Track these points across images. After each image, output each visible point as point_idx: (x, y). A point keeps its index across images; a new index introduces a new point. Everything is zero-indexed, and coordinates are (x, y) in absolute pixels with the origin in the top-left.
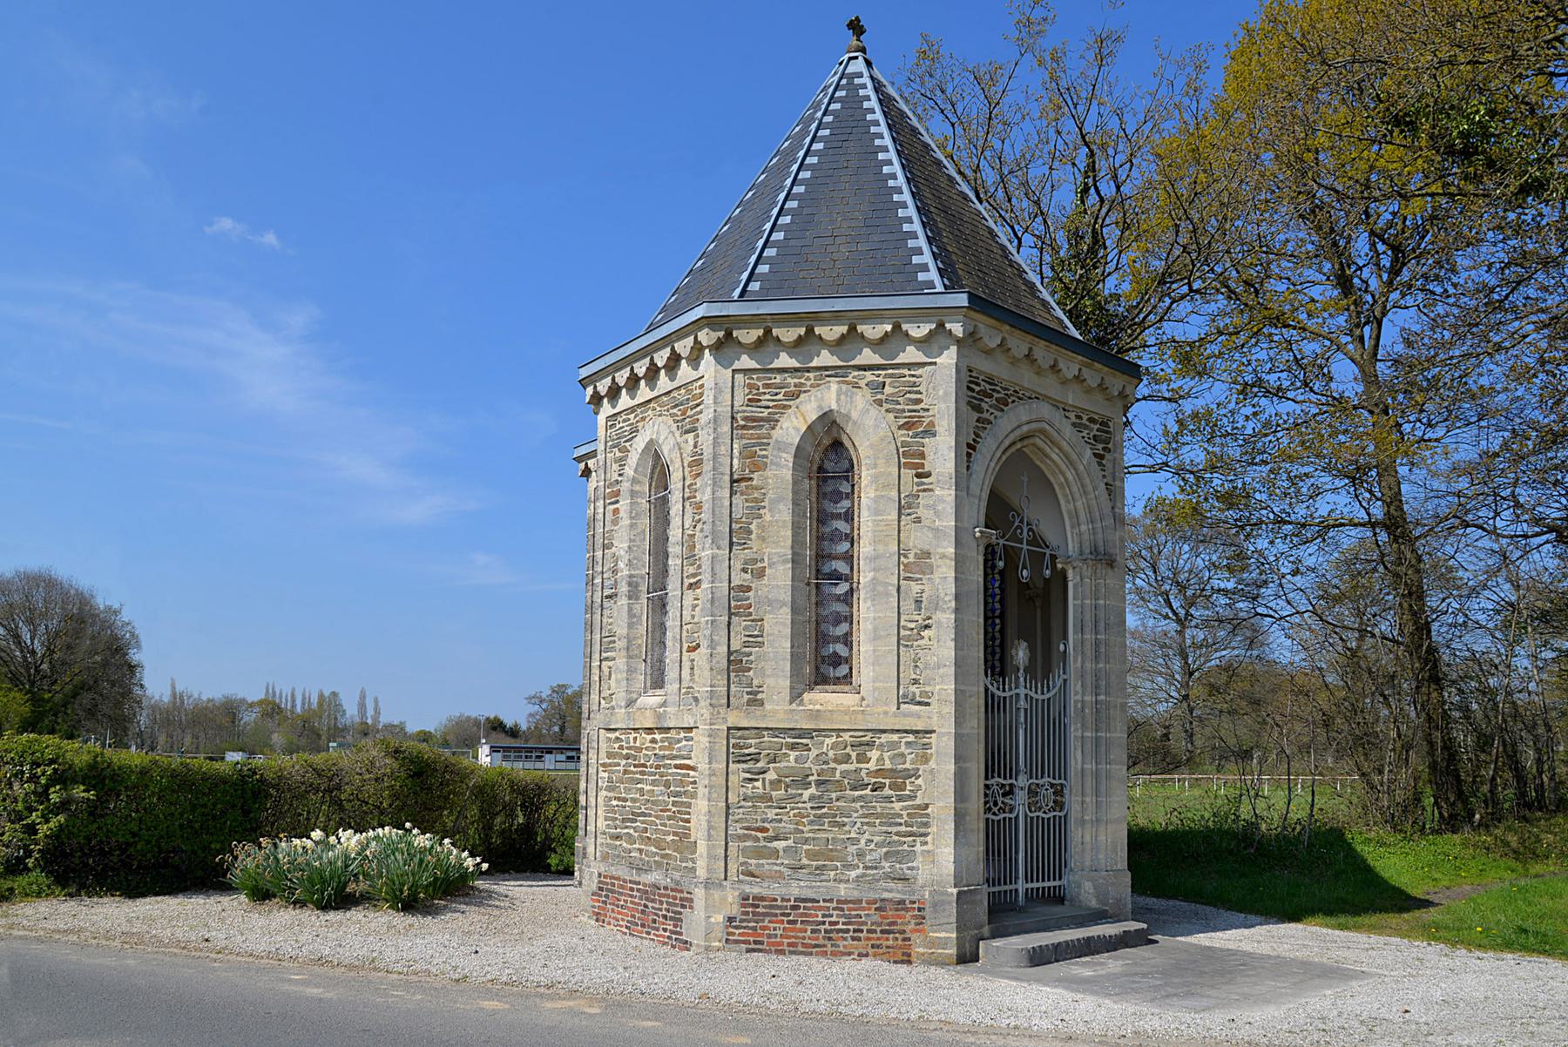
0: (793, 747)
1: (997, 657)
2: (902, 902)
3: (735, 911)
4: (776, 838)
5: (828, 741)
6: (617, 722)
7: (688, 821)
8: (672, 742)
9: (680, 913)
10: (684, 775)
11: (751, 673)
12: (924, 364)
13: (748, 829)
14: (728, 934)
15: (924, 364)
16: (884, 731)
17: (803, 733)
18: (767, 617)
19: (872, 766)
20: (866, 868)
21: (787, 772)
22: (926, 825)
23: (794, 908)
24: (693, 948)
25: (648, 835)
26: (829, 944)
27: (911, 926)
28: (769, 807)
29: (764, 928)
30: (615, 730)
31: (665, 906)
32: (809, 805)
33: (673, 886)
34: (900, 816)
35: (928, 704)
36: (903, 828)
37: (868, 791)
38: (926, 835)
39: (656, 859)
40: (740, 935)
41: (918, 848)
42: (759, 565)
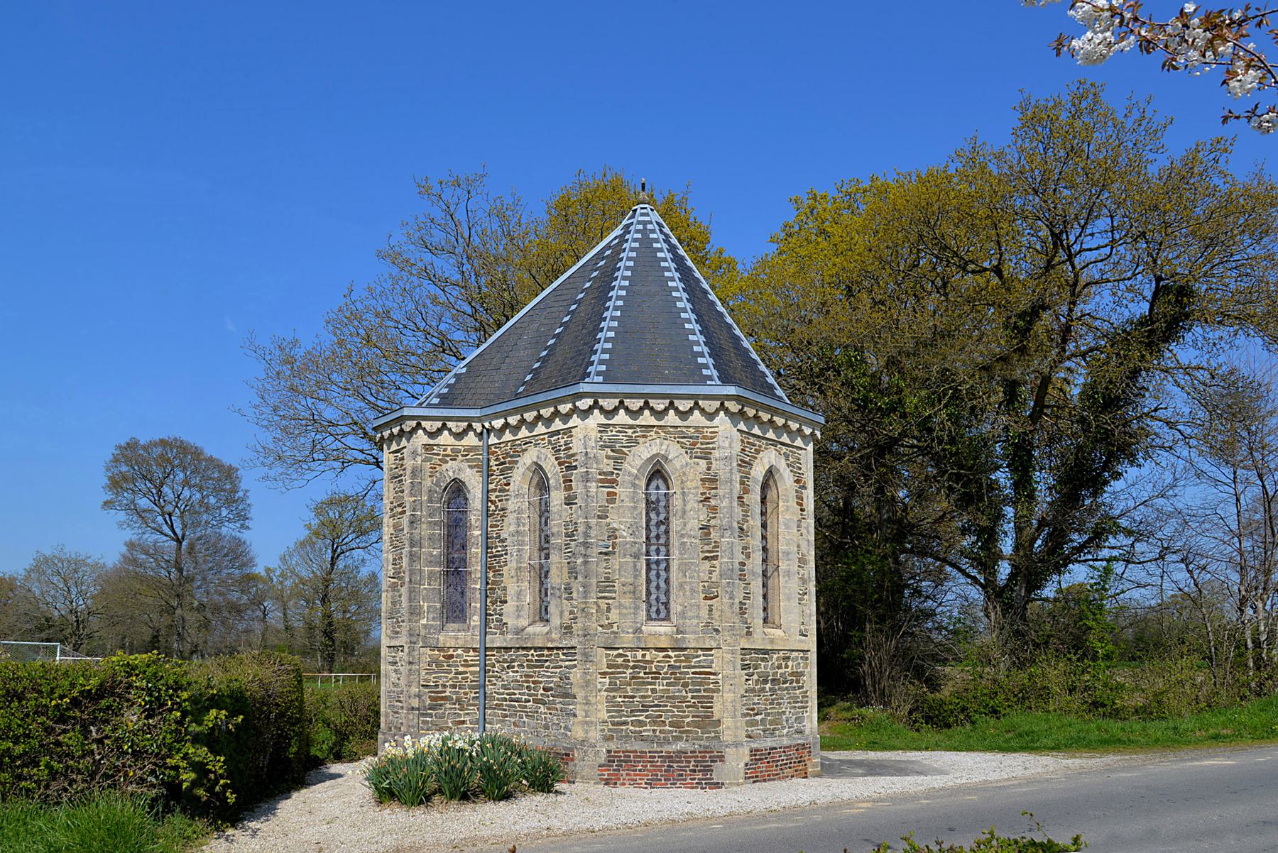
0: (762, 660)
1: (654, 609)
2: (804, 745)
3: (747, 759)
4: (757, 714)
5: (775, 656)
6: (624, 643)
7: (711, 707)
8: (688, 658)
9: (711, 766)
10: (704, 678)
11: (746, 616)
12: (802, 449)
13: (747, 709)
14: (747, 773)
15: (802, 449)
16: (793, 651)
17: (766, 652)
18: (752, 583)
19: (789, 670)
20: (789, 728)
21: (761, 674)
22: (807, 702)
23: (769, 754)
24: (149, 820)
25: (662, 719)
26: (781, 772)
27: (807, 758)
28: (755, 696)
29: (759, 767)
30: (618, 649)
31: (693, 763)
32: (769, 694)
33: (702, 749)
34: (798, 697)
35: (806, 636)
36: (800, 704)
37: (788, 685)
38: (807, 707)
39: (674, 734)
40: (751, 773)
41: (805, 714)
42: (748, 551)
